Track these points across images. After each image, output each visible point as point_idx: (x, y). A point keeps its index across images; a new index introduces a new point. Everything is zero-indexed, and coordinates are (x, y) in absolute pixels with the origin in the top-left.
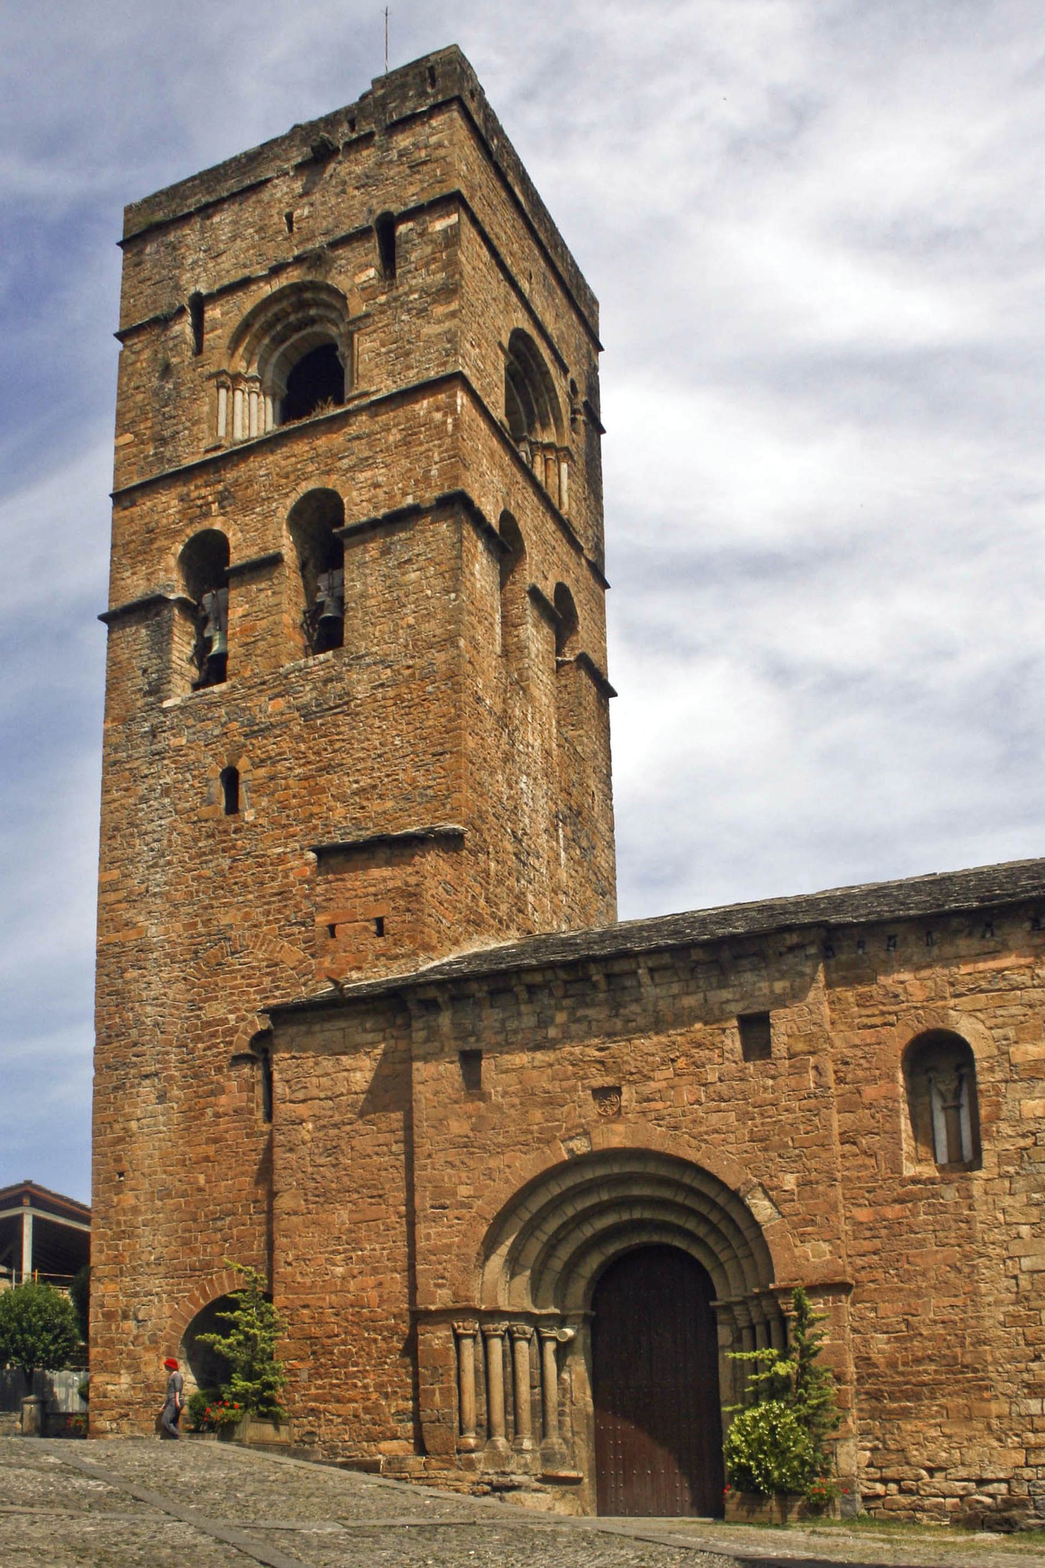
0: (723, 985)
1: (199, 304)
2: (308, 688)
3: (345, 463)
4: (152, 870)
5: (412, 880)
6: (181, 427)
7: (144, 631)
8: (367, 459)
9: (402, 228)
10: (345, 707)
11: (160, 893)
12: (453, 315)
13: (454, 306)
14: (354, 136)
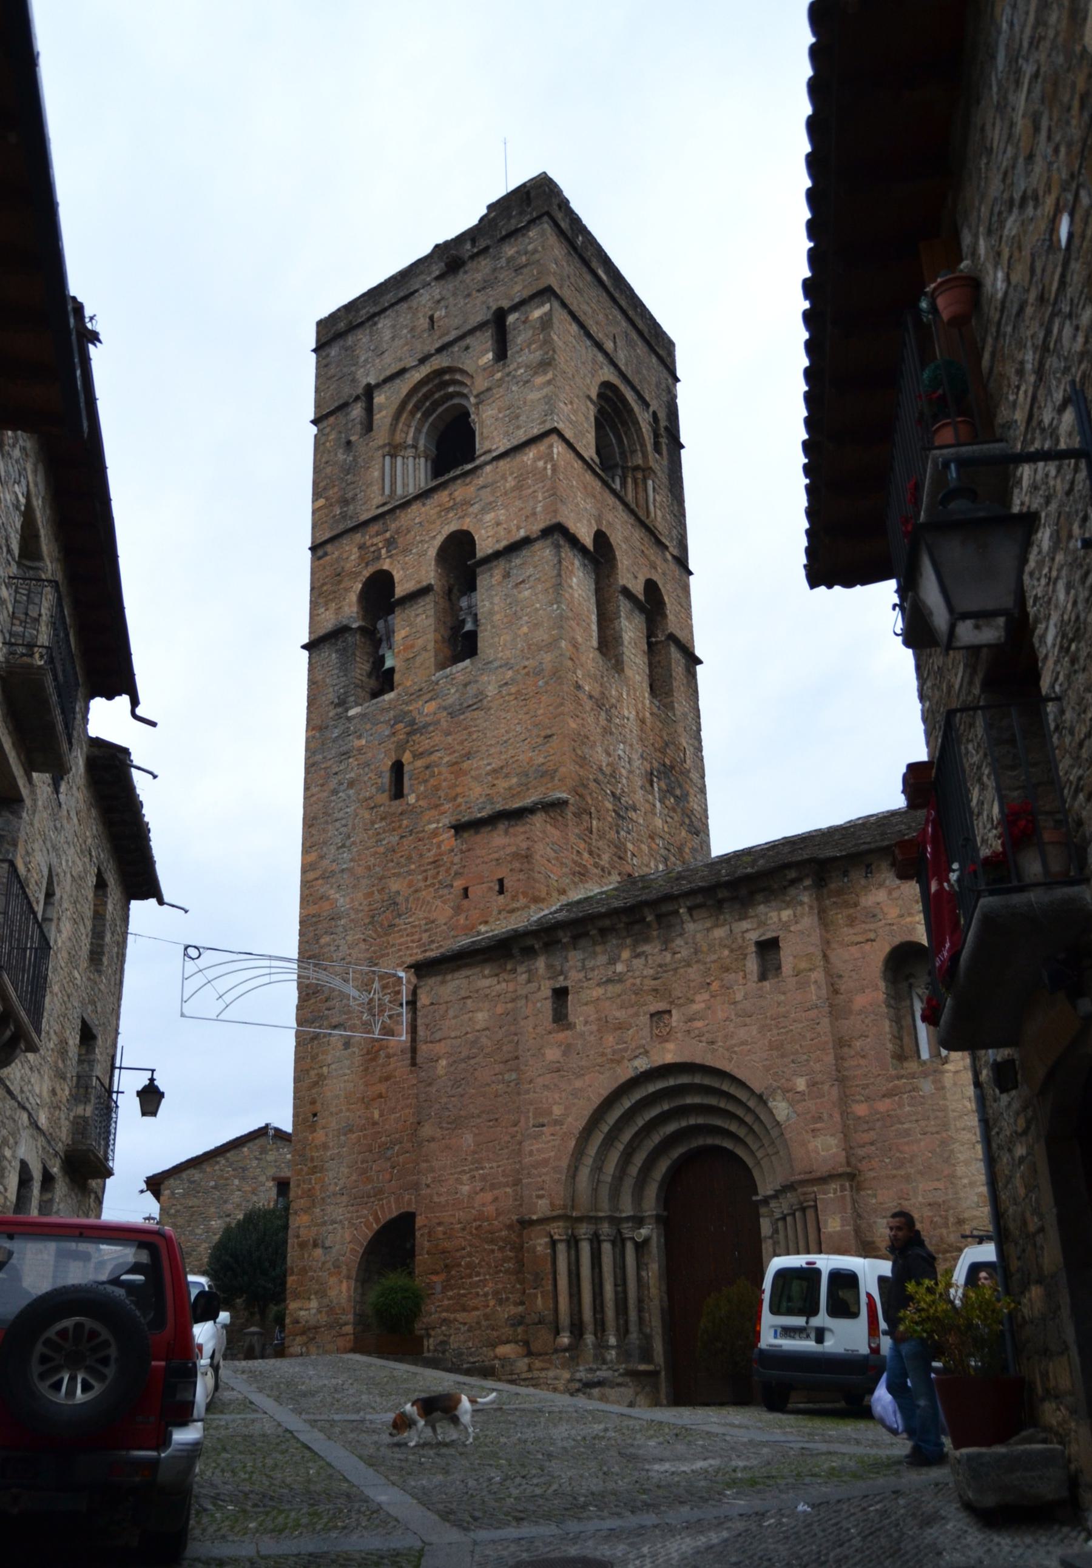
1: (369, 391)
2: (453, 691)
3: (476, 508)
4: (341, 851)
6: (358, 490)
7: (334, 655)
8: (491, 503)
10: (479, 704)
11: (347, 869)
12: (549, 382)
13: (549, 376)
14: (475, 250)
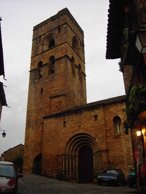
0: (92, 112)
1: (41, 36)
5: (60, 101)
9: (61, 27)
